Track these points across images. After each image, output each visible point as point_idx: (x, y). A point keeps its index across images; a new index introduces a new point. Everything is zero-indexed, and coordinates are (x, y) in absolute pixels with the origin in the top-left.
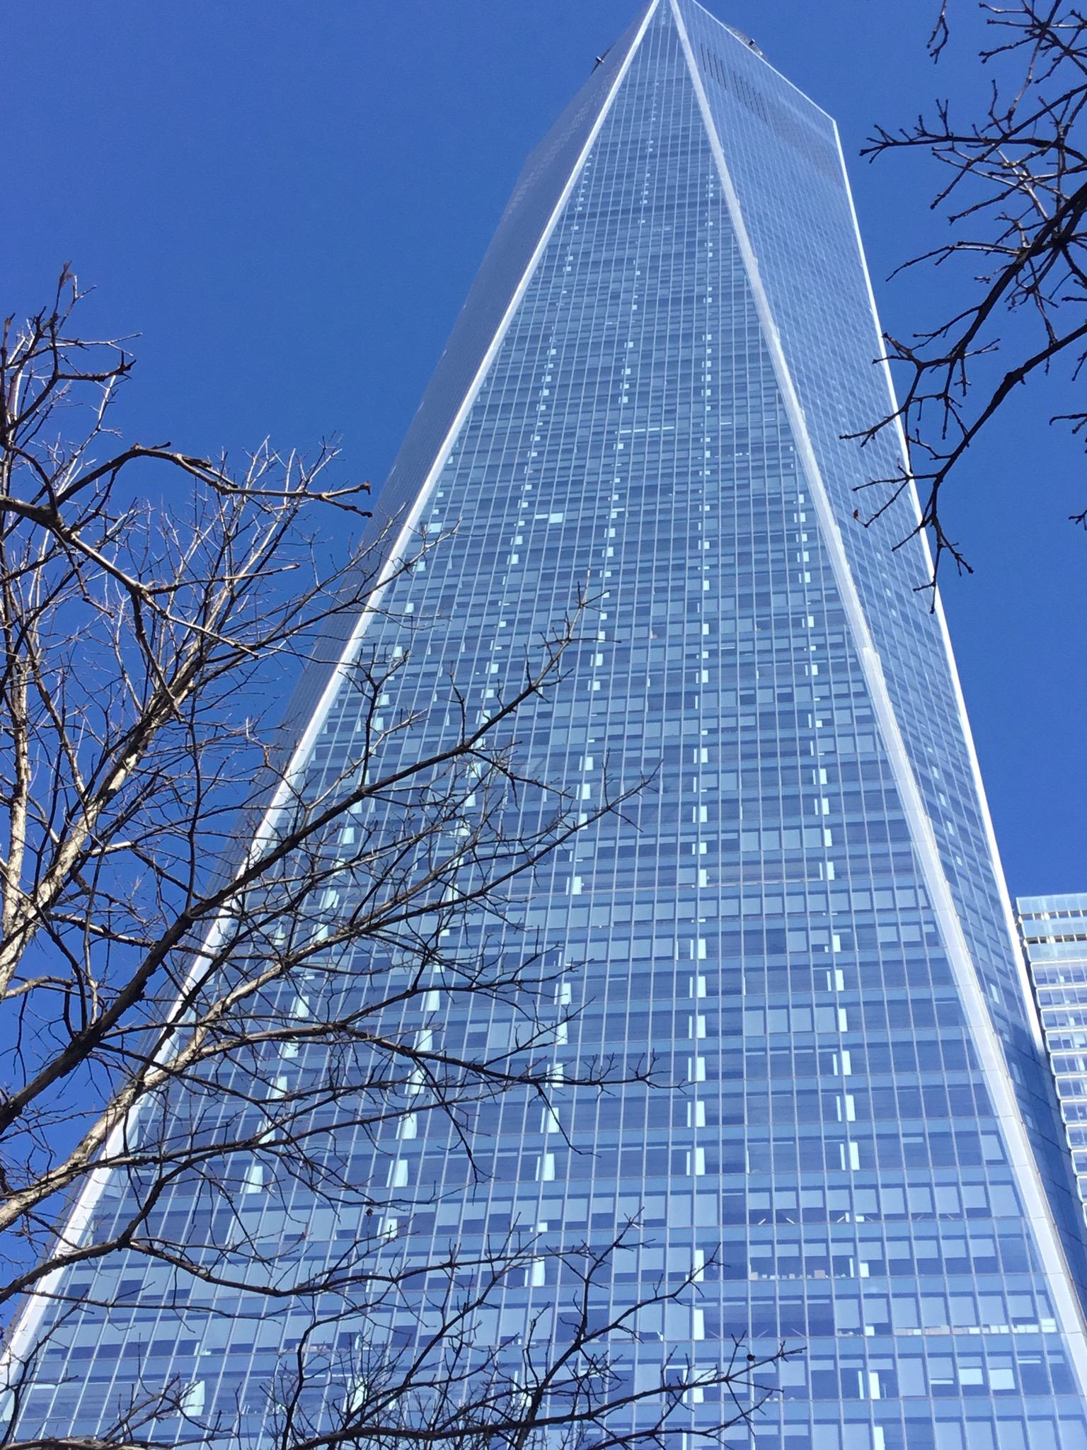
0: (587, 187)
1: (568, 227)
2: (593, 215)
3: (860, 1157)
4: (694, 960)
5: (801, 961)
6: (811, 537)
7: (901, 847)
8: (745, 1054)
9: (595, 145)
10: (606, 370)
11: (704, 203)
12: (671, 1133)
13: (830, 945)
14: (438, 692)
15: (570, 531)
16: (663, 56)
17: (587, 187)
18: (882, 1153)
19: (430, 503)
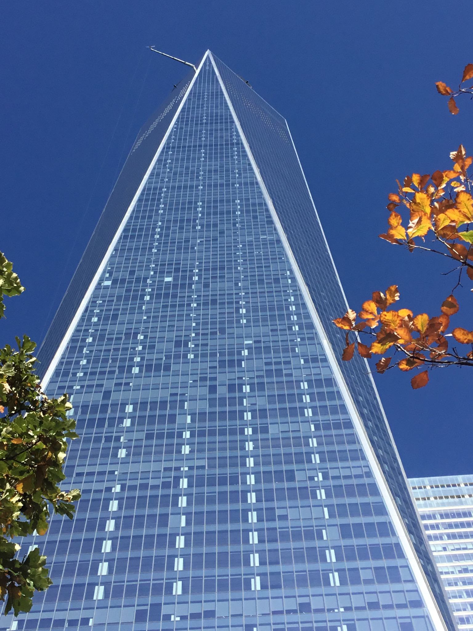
1: (167, 152)
3: (340, 581)
4: (250, 485)
5: (303, 485)
7: (349, 431)
8: (278, 530)
11: (232, 144)
12: (243, 570)
13: (318, 476)
14: (111, 358)
15: (175, 286)
16: (209, 82)
18: (351, 577)
19: (104, 272)
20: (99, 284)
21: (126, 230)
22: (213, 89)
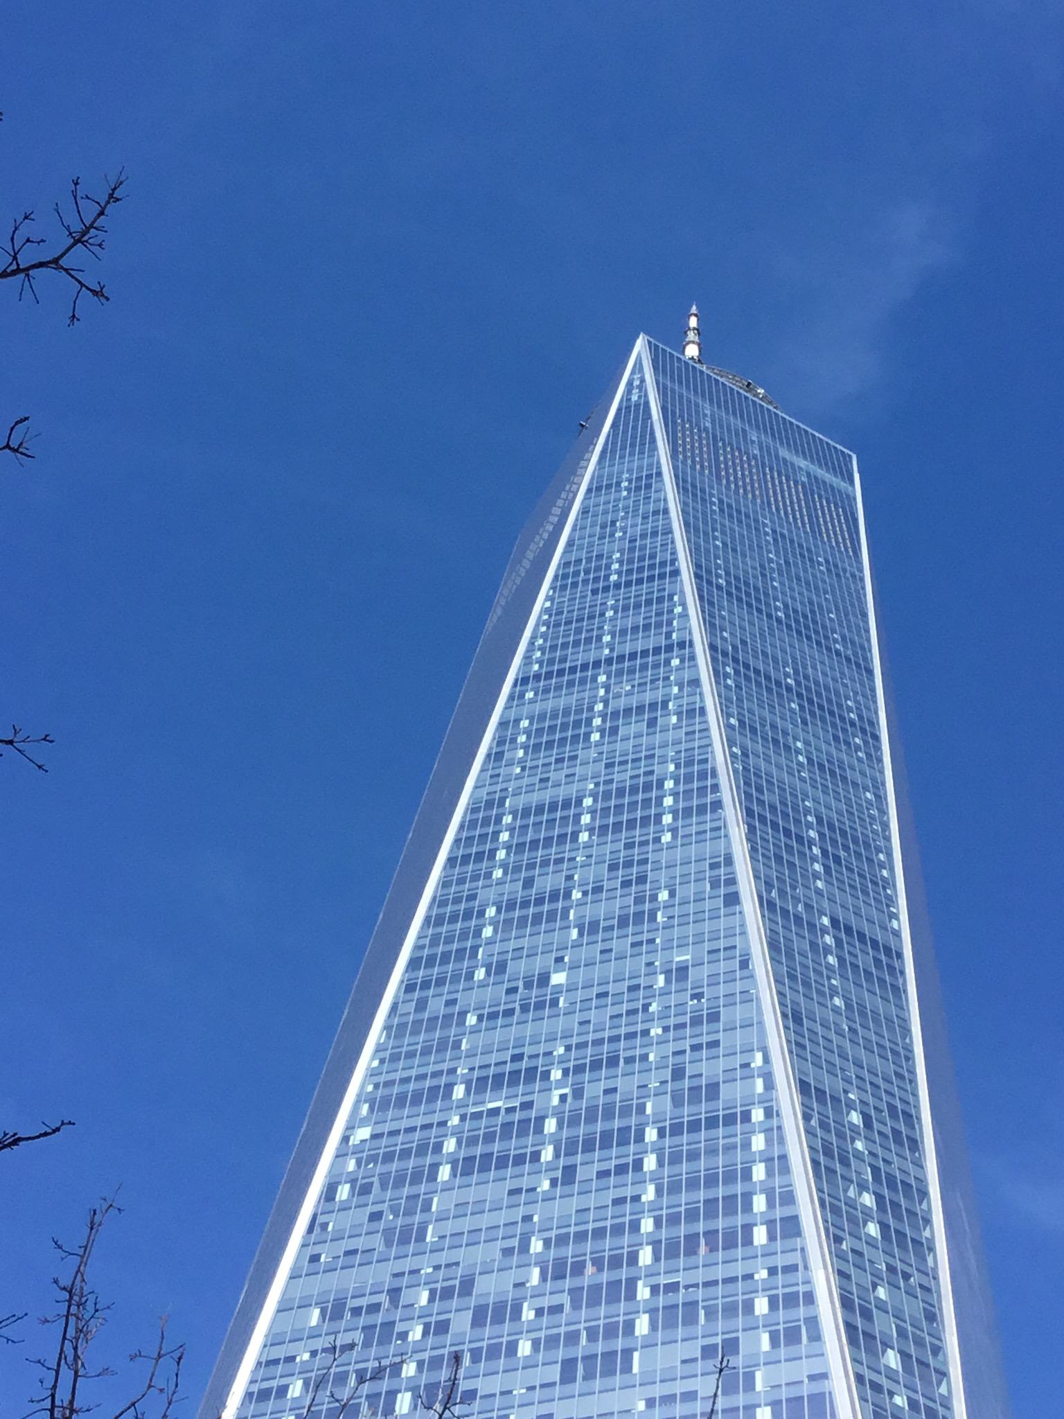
0: (544, 636)
1: (522, 696)
2: (549, 675)
6: (769, 1113)
9: (556, 577)
10: (554, 897)
16: (633, 445)
17: (544, 636)
19: (358, 1103)
20: (345, 1139)
21: (413, 964)
22: (640, 468)
